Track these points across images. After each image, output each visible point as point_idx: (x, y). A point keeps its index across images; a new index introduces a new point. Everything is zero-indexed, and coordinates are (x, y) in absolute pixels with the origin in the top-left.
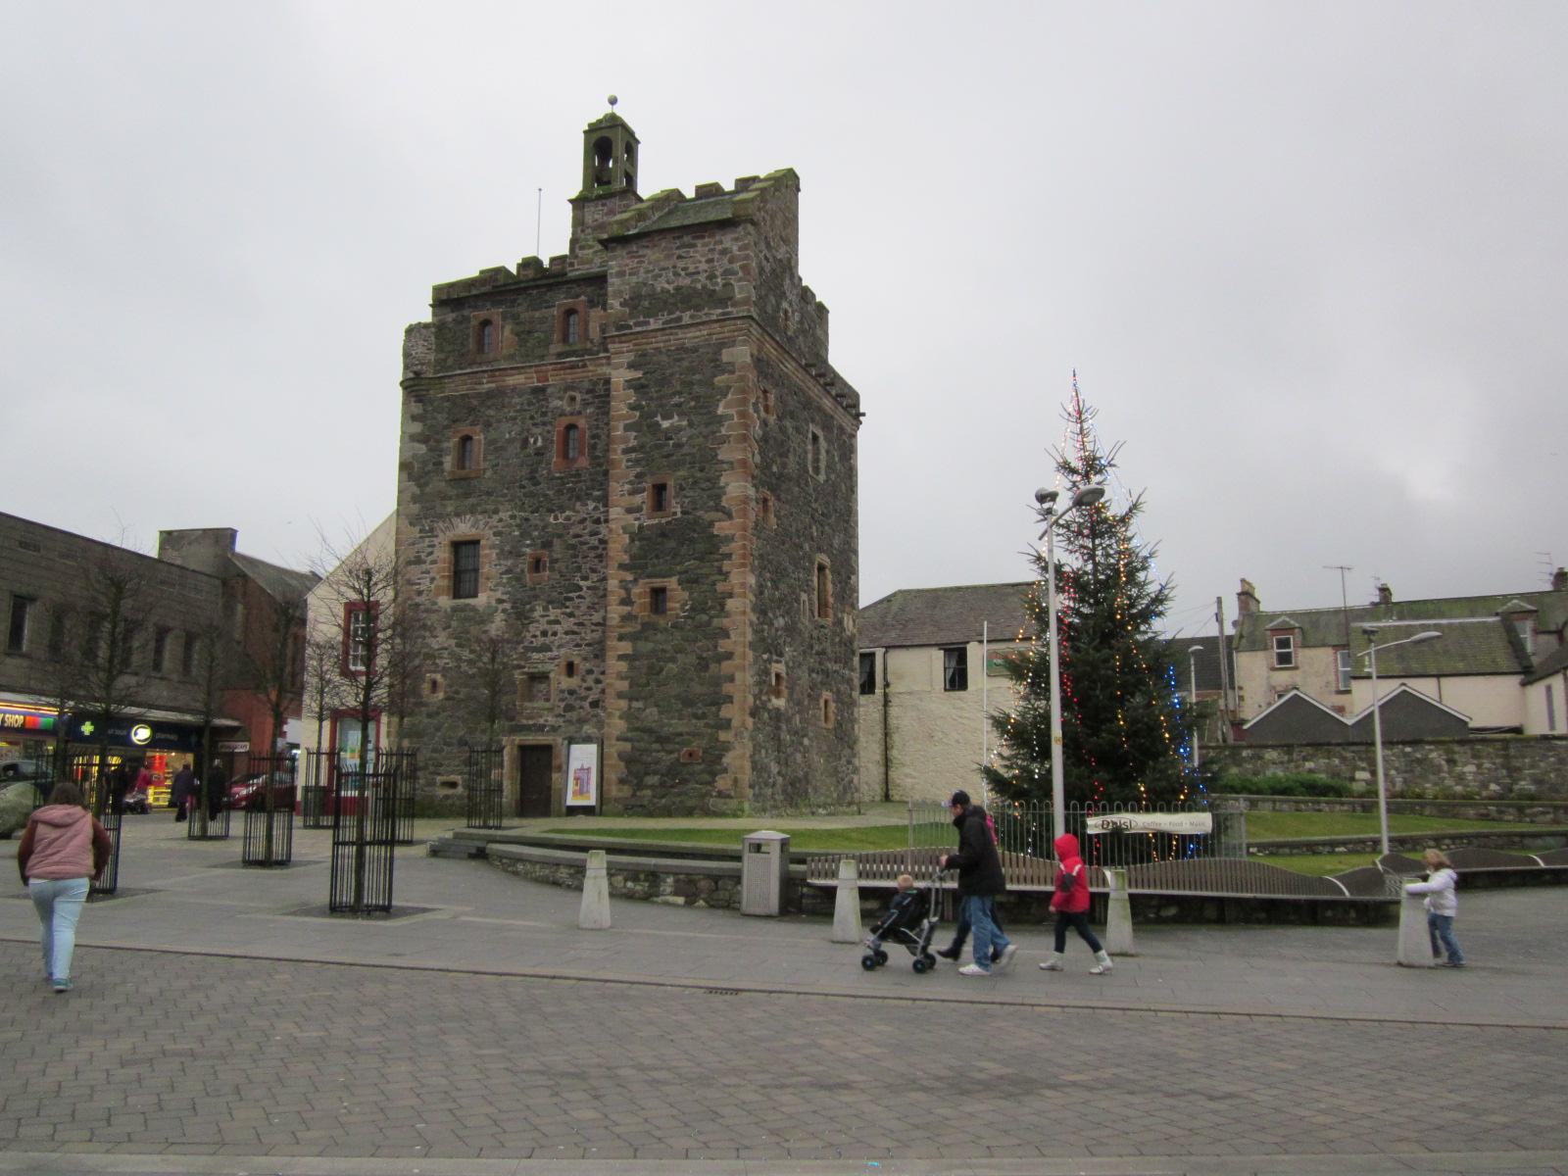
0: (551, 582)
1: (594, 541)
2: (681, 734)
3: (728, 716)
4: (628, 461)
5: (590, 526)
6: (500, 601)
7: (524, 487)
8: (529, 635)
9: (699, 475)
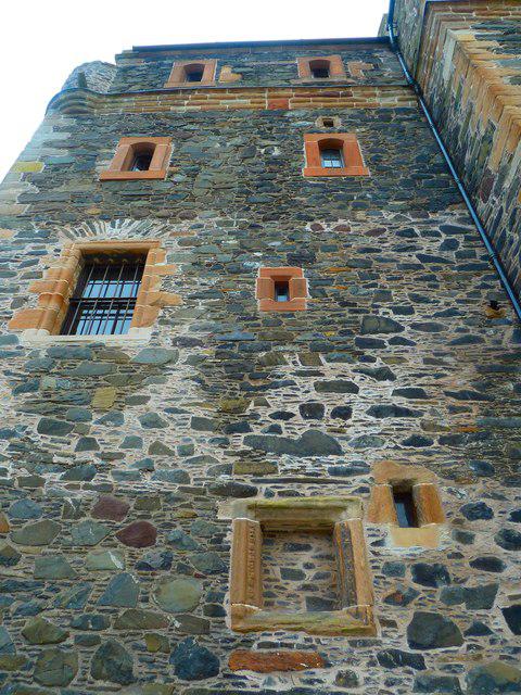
6: (187, 343)
8: (265, 414)
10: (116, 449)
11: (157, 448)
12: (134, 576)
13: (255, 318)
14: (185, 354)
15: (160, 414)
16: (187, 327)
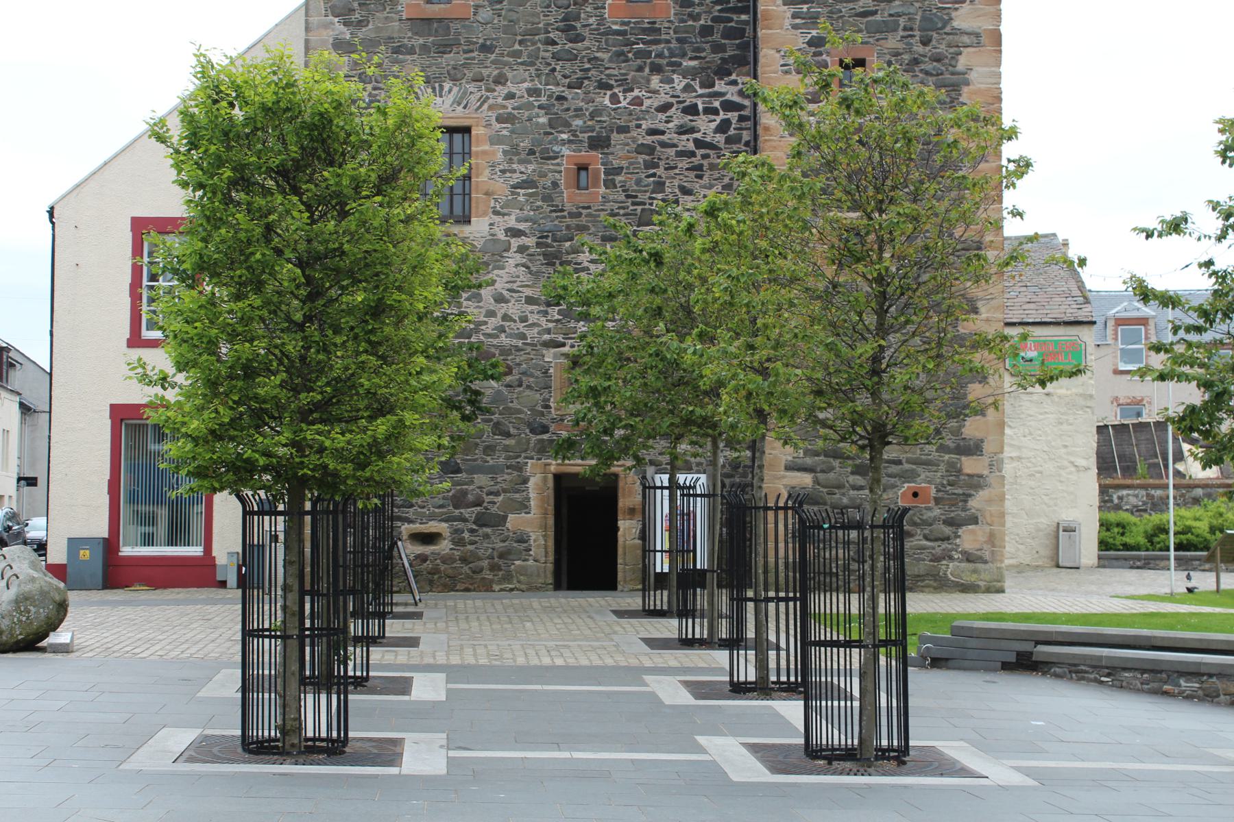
0: (608, 206)
1: (686, 142)
2: (899, 462)
3: (978, 435)
4: (794, 16)
5: (678, 118)
6: (516, 233)
7: (554, 43)
9: (920, 49)
10: (482, 319)
11: (506, 317)
12: (504, 390)
13: (562, 211)
14: (515, 243)
15: (505, 293)
16: (513, 217)
